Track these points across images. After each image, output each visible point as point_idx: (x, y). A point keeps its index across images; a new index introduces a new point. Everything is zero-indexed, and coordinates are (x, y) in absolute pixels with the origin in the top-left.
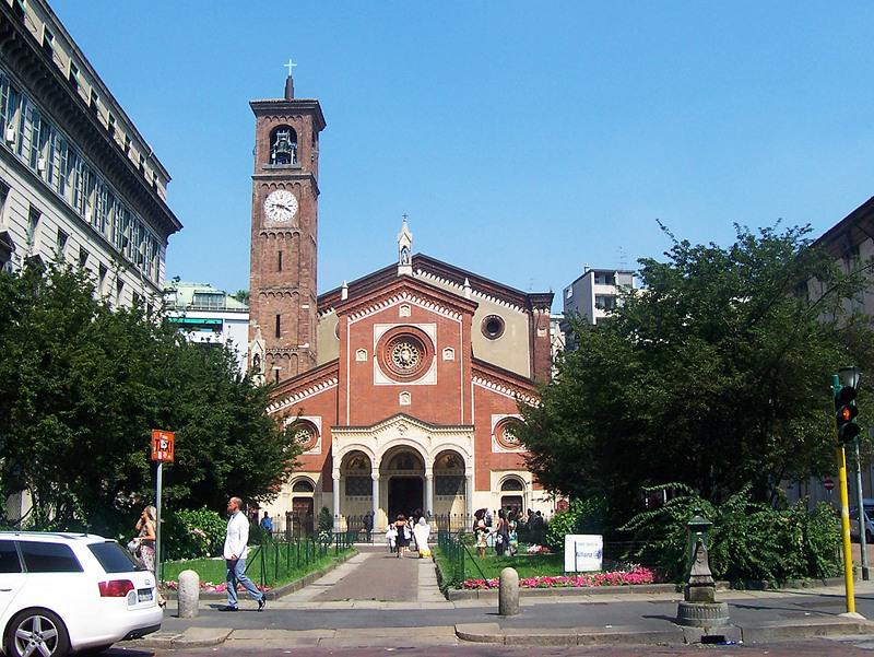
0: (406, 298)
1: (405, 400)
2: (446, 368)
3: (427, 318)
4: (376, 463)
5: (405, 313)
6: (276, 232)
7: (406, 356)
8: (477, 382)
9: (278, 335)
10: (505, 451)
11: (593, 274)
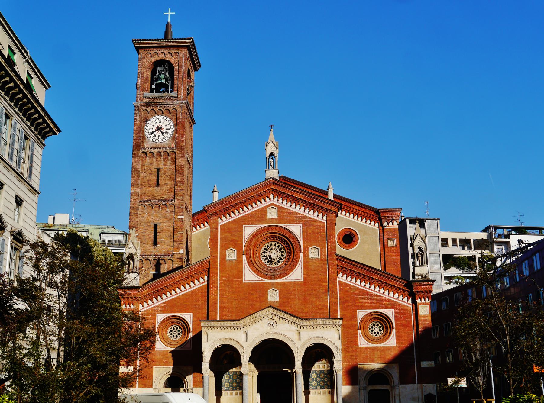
0: (273, 200)
1: (273, 296)
2: (312, 266)
3: (294, 218)
4: (245, 356)
5: (272, 214)
6: (155, 151)
7: (274, 255)
8: (342, 278)
9: (155, 243)
10: (371, 345)
11: (408, 220)
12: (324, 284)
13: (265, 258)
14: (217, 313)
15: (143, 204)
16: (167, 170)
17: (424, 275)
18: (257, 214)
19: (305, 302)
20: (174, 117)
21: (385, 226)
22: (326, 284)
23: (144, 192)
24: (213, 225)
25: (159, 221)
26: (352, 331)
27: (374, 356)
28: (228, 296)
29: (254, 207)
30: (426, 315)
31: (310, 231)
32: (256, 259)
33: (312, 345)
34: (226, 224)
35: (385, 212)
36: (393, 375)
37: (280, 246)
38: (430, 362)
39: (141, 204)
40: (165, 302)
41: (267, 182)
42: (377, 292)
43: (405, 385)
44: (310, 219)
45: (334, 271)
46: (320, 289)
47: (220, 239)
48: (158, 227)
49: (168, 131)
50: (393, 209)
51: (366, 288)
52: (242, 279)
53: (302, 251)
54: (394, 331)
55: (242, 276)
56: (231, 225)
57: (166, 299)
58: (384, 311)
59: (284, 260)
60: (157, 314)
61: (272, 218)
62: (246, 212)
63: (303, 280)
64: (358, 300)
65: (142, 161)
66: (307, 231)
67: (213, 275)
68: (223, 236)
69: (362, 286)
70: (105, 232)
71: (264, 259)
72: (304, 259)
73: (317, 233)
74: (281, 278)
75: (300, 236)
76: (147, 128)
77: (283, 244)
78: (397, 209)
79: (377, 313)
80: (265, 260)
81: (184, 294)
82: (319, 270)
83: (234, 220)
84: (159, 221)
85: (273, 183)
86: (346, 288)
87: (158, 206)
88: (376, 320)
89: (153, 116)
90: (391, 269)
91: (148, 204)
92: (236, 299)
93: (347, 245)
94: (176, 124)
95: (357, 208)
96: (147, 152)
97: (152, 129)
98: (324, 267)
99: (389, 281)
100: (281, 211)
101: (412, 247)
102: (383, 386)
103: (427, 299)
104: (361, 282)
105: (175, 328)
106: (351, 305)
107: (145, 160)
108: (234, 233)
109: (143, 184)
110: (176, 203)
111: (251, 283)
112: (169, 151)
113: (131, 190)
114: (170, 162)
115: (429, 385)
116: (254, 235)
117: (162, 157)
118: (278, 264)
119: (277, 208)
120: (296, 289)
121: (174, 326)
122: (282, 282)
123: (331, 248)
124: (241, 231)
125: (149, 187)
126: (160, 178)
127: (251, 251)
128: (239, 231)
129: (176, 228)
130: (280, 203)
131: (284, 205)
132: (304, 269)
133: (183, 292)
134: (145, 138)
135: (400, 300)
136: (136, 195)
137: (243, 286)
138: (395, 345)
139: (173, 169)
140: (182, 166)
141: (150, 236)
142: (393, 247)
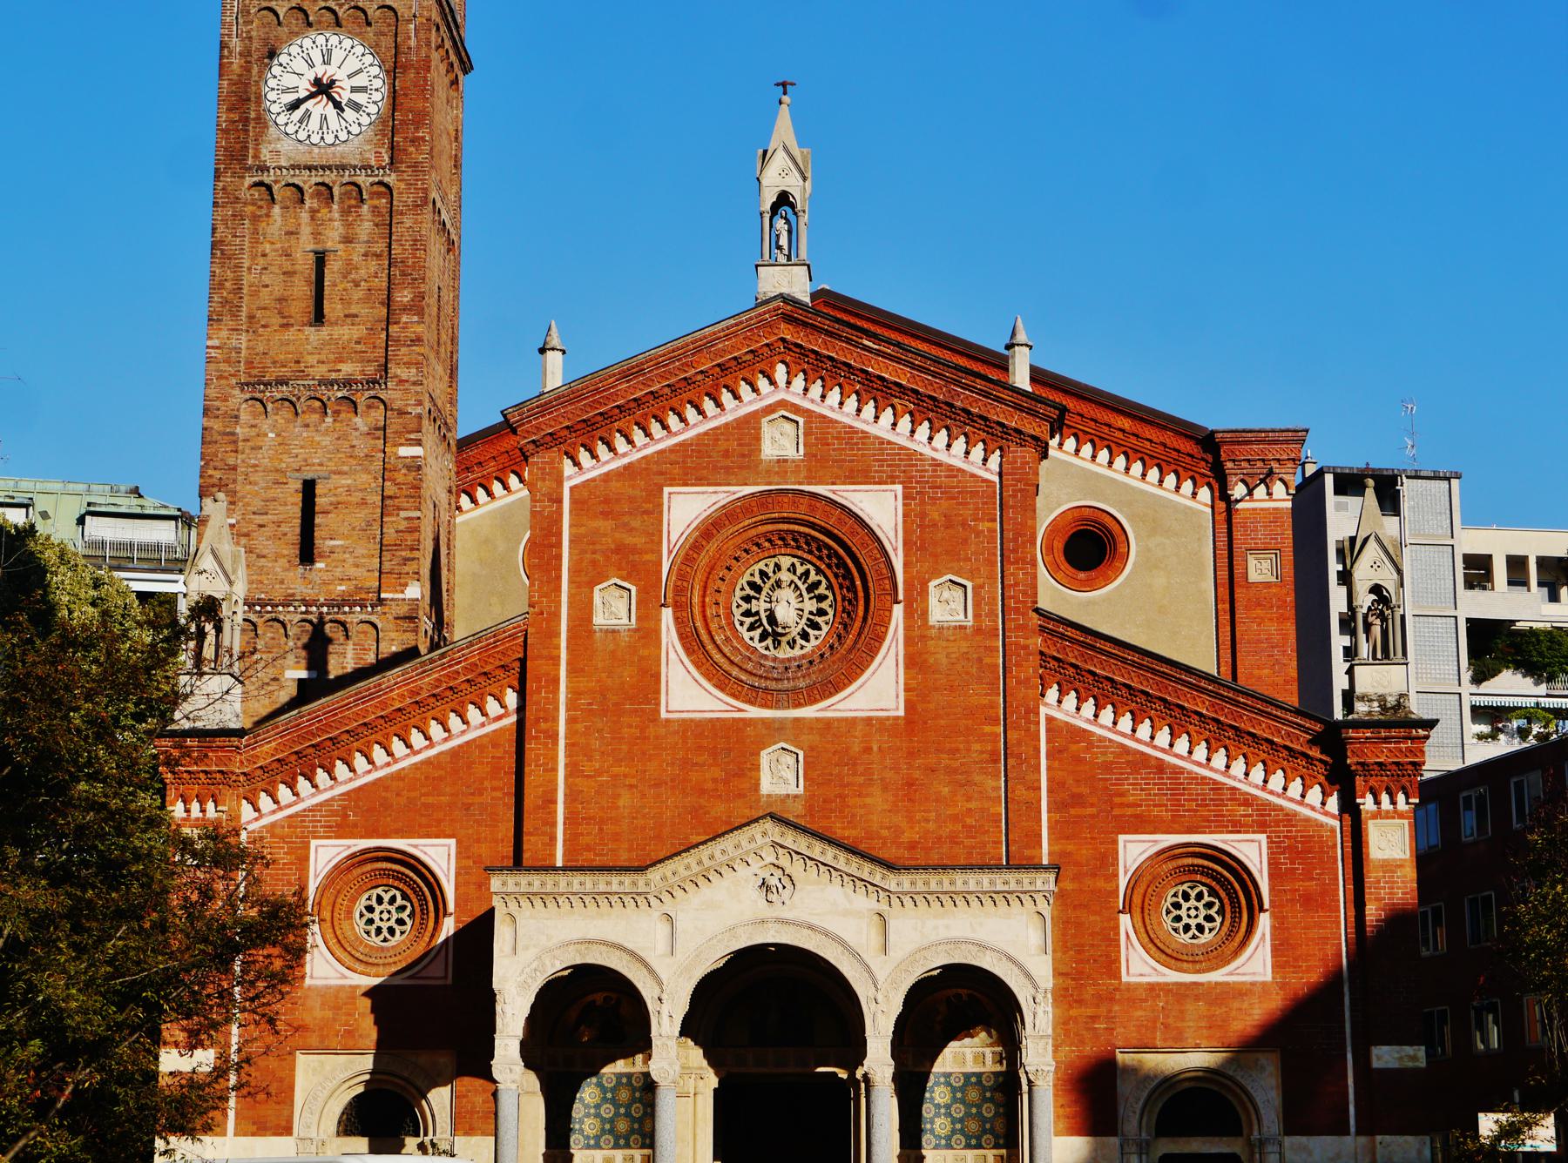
2: (940, 656)
6: (308, 181)
9: (307, 553)
10: (1173, 976)
11: (1329, 480)
12: (987, 729)
13: (752, 619)
14: (553, 838)
15: (258, 395)
16: (356, 258)
17: (1391, 701)
18: (722, 445)
19: (910, 800)
20: (387, 42)
21: (1238, 501)
22: (995, 729)
23: (261, 348)
24: (544, 487)
25: (321, 465)
26: (1098, 918)
27: (1183, 1020)
28: (599, 773)
29: (709, 414)
30: (1395, 860)
31: (936, 516)
32: (713, 626)
33: (935, 973)
34: (593, 480)
35: (1239, 443)
36: (1259, 1098)
37: (813, 573)
38: (1409, 1050)
39: (248, 396)
40: (347, 793)
41: (765, 313)
42: (1199, 764)
43: (1303, 1139)
44: (937, 464)
45: (1027, 680)
46: (969, 750)
47: (571, 541)
48: (319, 489)
49: (360, 98)
50: (1273, 431)
51: (1155, 747)
52: (658, 704)
53: (901, 597)
54: (1264, 922)
55: (658, 692)
56: (614, 485)
57: (351, 780)
58: (1224, 842)
59: (825, 628)
60: (314, 843)
61: (782, 462)
62: (676, 434)
63: (901, 713)
64: (1122, 795)
65: (255, 219)
66: (923, 515)
67: (539, 691)
68: (582, 530)
69: (1139, 741)
70: (103, 509)
71: (746, 626)
72: (908, 628)
73: (964, 524)
74: (815, 701)
75: (891, 535)
76: (272, 83)
77: (823, 567)
78: (1288, 431)
79: (1197, 849)
80: (751, 628)
81: (422, 763)
82: (967, 673)
83: (627, 467)
84: (321, 465)
85: (788, 318)
86: (1074, 747)
87: (318, 404)
88: (1193, 877)
89: (297, 34)
90: (1256, 672)
91: (279, 396)
92: (631, 786)
93: (1082, 575)
94: (394, 69)
95: (1125, 423)
96: (276, 182)
97: (295, 89)
98: (987, 660)
99: (1250, 719)
100: (818, 431)
101: (1344, 589)
102: (1217, 1139)
103: (1401, 798)
104: (1136, 721)
105: (386, 897)
106: (1092, 816)
107: (268, 215)
108: (626, 519)
109: (259, 314)
110: (391, 394)
111: (692, 720)
112: (363, 180)
113: (210, 338)
114: (367, 226)
115: (1401, 1139)
116: (709, 529)
117: (335, 207)
118: (802, 647)
119: (801, 421)
120: (875, 748)
121: (379, 891)
122: (818, 719)
123: (1016, 584)
124: (653, 510)
125: (286, 326)
126: (326, 292)
127: (696, 593)
128: (647, 512)
129: (390, 497)
130: (812, 401)
131: (832, 408)
132: (907, 667)
133: (419, 752)
134: (267, 127)
135: (1291, 800)
136: (227, 361)
137: (663, 731)
138: (1268, 977)
139: (378, 256)
140: (418, 243)
141: (284, 528)
142: (1267, 585)
